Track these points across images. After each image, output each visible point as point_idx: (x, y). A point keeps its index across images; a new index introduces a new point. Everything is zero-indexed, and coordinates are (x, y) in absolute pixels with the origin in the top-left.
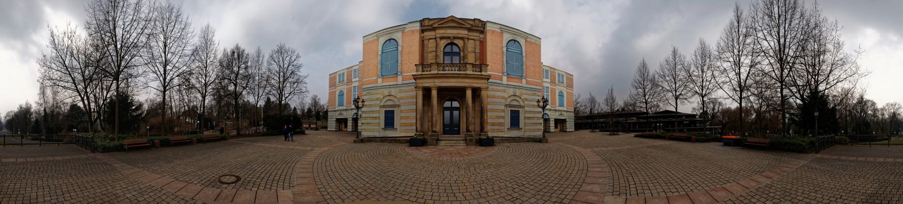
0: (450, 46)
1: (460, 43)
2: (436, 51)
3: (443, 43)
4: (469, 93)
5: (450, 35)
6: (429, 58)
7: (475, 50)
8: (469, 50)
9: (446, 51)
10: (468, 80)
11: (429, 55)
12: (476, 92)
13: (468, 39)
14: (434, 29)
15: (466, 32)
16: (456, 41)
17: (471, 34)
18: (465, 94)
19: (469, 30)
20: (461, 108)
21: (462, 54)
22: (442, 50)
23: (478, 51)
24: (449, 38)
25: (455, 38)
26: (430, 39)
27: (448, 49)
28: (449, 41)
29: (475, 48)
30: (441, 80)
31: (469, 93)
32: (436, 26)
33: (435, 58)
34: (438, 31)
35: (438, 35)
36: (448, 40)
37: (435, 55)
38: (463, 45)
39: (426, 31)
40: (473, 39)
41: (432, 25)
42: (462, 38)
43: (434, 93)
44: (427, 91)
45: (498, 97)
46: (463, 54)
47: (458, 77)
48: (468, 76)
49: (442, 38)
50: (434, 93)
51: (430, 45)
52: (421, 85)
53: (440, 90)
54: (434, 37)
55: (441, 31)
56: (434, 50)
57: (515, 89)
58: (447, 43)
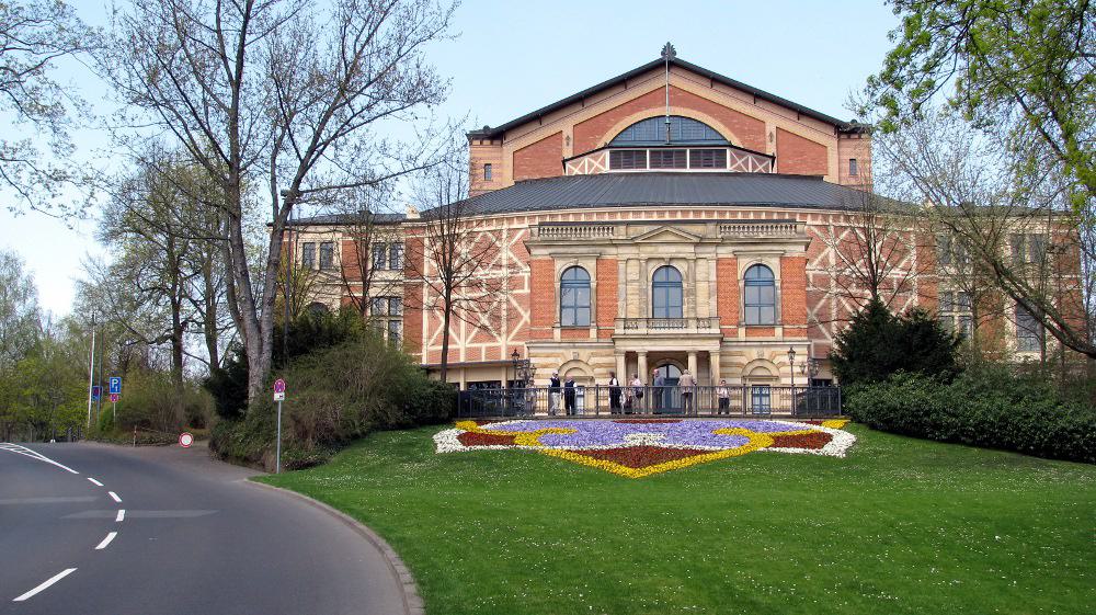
1: (682, 267)
3: (652, 267)
4: (692, 360)
5: (664, 256)
9: (657, 279)
10: (690, 342)
15: (692, 249)
16: (674, 264)
17: (700, 249)
19: (696, 245)
21: (685, 285)
23: (713, 278)
24: (663, 259)
27: (661, 277)
29: (708, 274)
30: (652, 343)
31: (692, 360)
34: (642, 249)
43: (642, 360)
47: (676, 339)
49: (650, 259)
50: (642, 360)
52: (624, 349)
53: (650, 355)
55: (649, 249)
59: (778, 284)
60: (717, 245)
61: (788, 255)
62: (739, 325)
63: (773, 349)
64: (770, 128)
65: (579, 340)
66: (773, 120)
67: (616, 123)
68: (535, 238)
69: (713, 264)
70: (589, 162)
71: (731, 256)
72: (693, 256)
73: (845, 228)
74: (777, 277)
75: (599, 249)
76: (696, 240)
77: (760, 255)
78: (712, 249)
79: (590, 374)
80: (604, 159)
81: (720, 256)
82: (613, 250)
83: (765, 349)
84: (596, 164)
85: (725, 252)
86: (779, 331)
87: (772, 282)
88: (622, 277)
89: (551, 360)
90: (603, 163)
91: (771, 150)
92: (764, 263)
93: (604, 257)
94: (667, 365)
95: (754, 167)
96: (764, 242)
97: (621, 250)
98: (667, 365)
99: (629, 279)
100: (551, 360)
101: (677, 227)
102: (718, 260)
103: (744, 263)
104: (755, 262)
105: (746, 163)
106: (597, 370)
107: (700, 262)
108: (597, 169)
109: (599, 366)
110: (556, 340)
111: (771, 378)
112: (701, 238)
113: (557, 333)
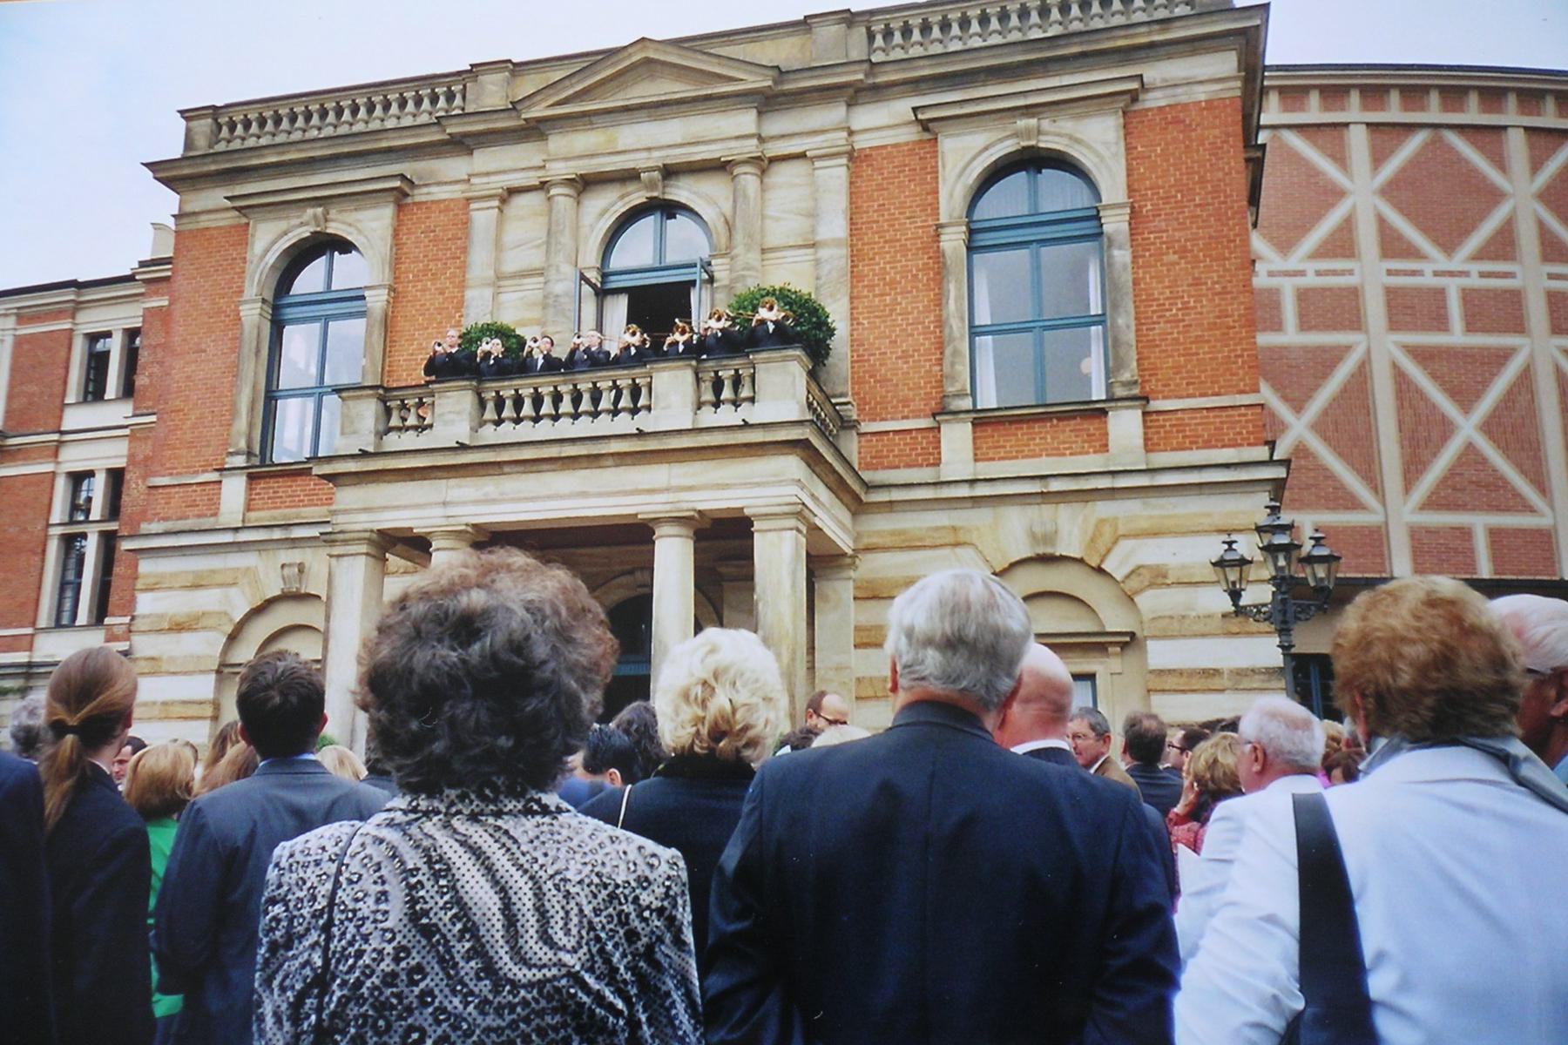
0: (648, 224)
10: (658, 474)
13: (764, 164)
14: (535, 130)
15: (745, 121)
16: (681, 191)
22: (590, 258)
24: (629, 176)
25: (670, 172)
26: (513, 192)
28: (638, 197)
29: (813, 215)
34: (559, 143)
36: (631, 187)
37: (539, 294)
38: (727, 208)
39: (482, 145)
40: (802, 156)
41: (515, 107)
47: (594, 460)
48: (652, 445)
49: (585, 184)
54: (532, 179)
57: (1047, 510)
58: (622, 208)
59: (1115, 224)
60: (856, 95)
61: (1153, 100)
62: (942, 411)
63: (1104, 509)
69: (835, 175)
71: (911, 134)
72: (751, 147)
73: (1411, 127)
74: (1113, 187)
77: (1028, 110)
78: (833, 114)
81: (862, 142)
82: (454, 167)
86: (1125, 426)
87: (1088, 225)
88: (480, 261)
89: (206, 600)
92: (1046, 143)
93: (420, 195)
97: (485, 159)
99: (510, 266)
100: (206, 600)
102: (855, 158)
104: (1009, 146)
107: (783, 175)
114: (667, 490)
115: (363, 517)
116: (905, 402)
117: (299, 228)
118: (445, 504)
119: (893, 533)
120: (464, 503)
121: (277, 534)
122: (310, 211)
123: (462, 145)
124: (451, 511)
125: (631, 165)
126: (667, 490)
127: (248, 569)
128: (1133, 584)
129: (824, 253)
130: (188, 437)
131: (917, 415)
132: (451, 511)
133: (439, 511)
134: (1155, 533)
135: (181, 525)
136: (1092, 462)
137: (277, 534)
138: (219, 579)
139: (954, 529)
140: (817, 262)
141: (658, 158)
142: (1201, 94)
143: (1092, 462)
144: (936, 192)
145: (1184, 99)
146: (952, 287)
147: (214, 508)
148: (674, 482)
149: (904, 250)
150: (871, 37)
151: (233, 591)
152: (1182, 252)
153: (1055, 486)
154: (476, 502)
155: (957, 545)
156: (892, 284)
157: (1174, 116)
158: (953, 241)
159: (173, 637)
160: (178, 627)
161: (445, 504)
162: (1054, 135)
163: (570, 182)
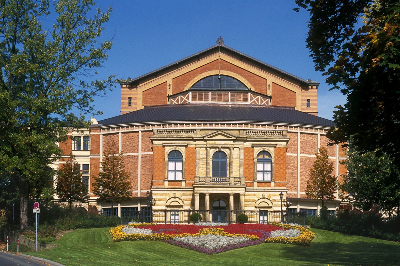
1: (227, 151)
2: (207, 158)
4: (232, 198)
6: (200, 164)
7: (240, 157)
8: (235, 157)
11: (200, 161)
12: (237, 197)
16: (223, 150)
17: (237, 143)
18: (229, 198)
19: (234, 141)
20: (227, 207)
23: (242, 157)
24: (217, 147)
25: (222, 147)
26: (201, 147)
31: (232, 198)
32: (206, 138)
33: (205, 164)
35: (208, 146)
38: (229, 153)
40: (238, 147)
42: (229, 148)
43: (208, 198)
44: (202, 196)
45: (249, 200)
46: (230, 161)
50: (208, 198)
51: (201, 153)
53: (211, 195)
56: (205, 157)
58: (215, 151)
60: (245, 141)
62: (254, 181)
64: (269, 82)
65: (177, 187)
66: (270, 79)
67: (194, 77)
68: (155, 136)
69: (242, 150)
70: (181, 97)
71: (251, 146)
74: (273, 157)
75: (186, 142)
76: (235, 139)
79: (182, 204)
80: (188, 96)
81: (245, 146)
83: (266, 193)
84: (185, 99)
85: (248, 144)
86: (273, 184)
89: (163, 197)
90: (188, 98)
91: (269, 93)
94: (219, 200)
95: (262, 102)
96: (266, 140)
97: (198, 142)
98: (219, 200)
100: (163, 197)
101: (225, 131)
103: (257, 150)
105: (257, 100)
106: (185, 202)
108: (185, 101)
109: (186, 200)
110: (165, 187)
111: (269, 207)
112: (237, 138)
113: (166, 183)
114: (231, 191)
115: (198, 191)
116: (250, 179)
117: (172, 148)
118: (208, 190)
119: (248, 194)
120: (210, 191)
121: (173, 189)
122: (175, 147)
123: (195, 141)
124: (208, 191)
125: (218, 146)
126: (231, 191)
127: (168, 193)
128: (273, 201)
129: (241, 160)
130: (158, 175)
131: (250, 181)
132: (208, 191)
133: (207, 191)
134: (275, 196)
135: (158, 187)
136: (269, 188)
137: (173, 189)
138: (165, 194)
139: (254, 194)
140: (240, 161)
141: (221, 146)
142: (283, 146)
143: (269, 188)
144: (254, 154)
145: (281, 147)
146: (255, 166)
147: (164, 185)
148: (232, 190)
149: (250, 161)
150: (246, 132)
151: (167, 196)
152: (279, 165)
153: (265, 190)
154: (211, 190)
155: (255, 196)
156: (248, 165)
157: (280, 149)
158: (256, 160)
159: (159, 201)
160: (160, 200)
161: (208, 190)
162: (267, 149)
163: (209, 148)
